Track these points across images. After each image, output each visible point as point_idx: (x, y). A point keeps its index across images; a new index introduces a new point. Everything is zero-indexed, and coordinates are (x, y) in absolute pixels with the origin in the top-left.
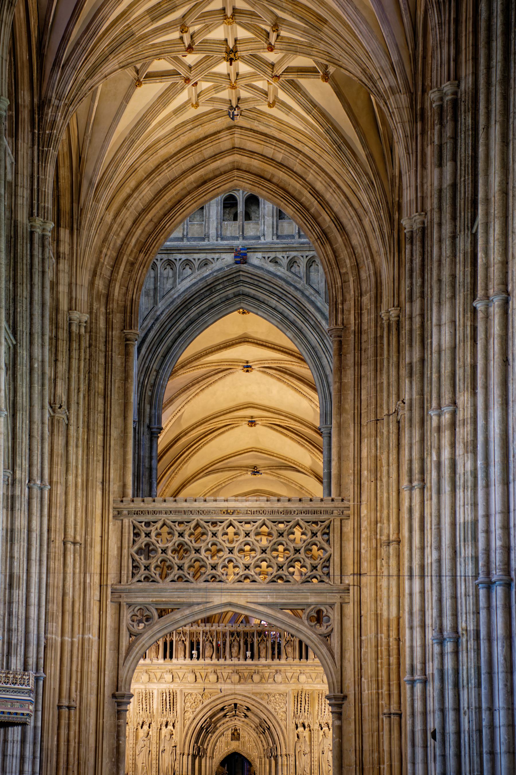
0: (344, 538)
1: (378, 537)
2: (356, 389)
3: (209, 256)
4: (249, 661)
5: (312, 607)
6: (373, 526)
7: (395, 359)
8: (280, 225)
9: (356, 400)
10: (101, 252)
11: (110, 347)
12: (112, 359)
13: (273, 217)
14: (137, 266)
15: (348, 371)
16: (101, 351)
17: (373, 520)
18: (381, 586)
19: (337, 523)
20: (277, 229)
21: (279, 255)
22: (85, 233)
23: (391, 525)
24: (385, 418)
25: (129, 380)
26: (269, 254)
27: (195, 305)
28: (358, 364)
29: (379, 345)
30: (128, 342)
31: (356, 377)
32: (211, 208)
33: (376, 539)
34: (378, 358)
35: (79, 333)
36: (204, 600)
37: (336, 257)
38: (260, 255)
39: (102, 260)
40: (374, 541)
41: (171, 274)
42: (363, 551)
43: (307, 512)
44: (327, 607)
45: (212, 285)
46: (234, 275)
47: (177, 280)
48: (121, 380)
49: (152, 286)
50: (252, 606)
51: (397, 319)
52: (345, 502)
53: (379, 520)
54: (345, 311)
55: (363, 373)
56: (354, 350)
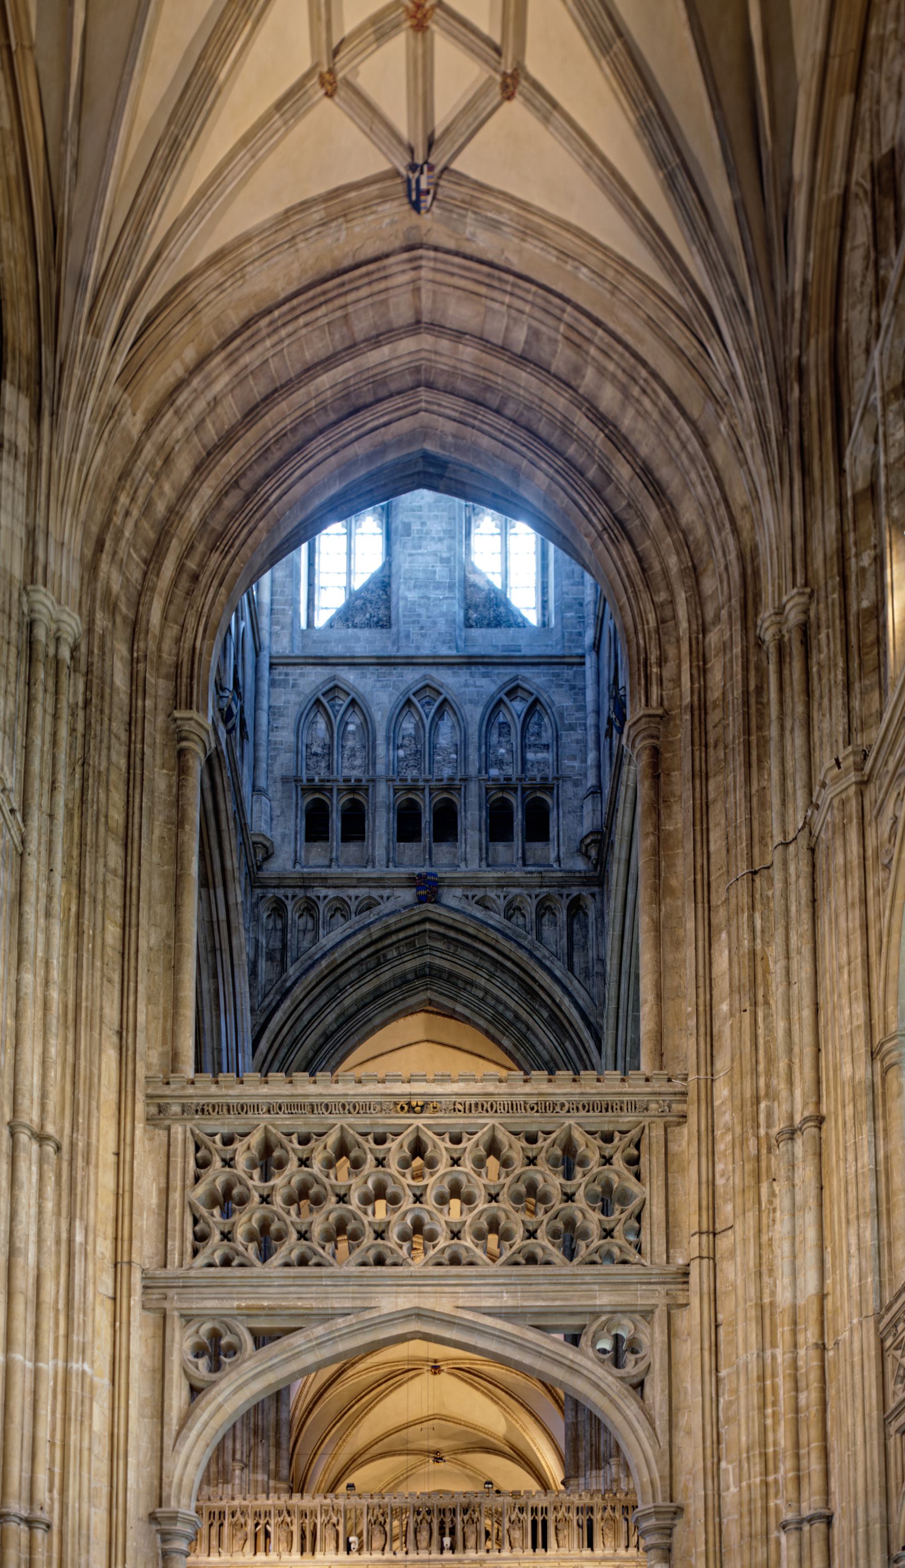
0: (673, 1167)
1: (762, 1132)
2: (698, 828)
3: (375, 893)
4: (448, 1555)
5: (604, 1318)
6: (748, 1109)
7: (800, 709)
8: (490, 848)
9: (699, 853)
10: (115, 500)
11: (139, 731)
12: (142, 760)
13: (480, 831)
14: (204, 580)
15: (676, 808)
16: (118, 738)
17: (748, 1094)
18: (770, 1240)
19: (657, 1133)
20: (487, 853)
21: (492, 894)
22: (68, 417)
23: (798, 1093)
24: (776, 857)
25: (187, 827)
26: (475, 891)
27: (352, 983)
28: (701, 776)
29: (753, 710)
30: (184, 744)
31: (698, 802)
32: (377, 814)
33: (758, 1138)
34: (753, 738)
35: (56, 656)
36: (358, 1303)
37: (644, 570)
38: (459, 892)
39: (117, 520)
40: (752, 1143)
41: (310, 925)
42: (720, 1181)
43: (588, 1107)
44: (637, 1317)
45: (380, 945)
46: (417, 929)
47: (321, 930)
48: (166, 822)
49: (278, 945)
50: (469, 1316)
51: (802, 617)
52: (677, 1082)
53: (762, 1092)
54: (665, 683)
55: (712, 796)
56: (693, 744)
